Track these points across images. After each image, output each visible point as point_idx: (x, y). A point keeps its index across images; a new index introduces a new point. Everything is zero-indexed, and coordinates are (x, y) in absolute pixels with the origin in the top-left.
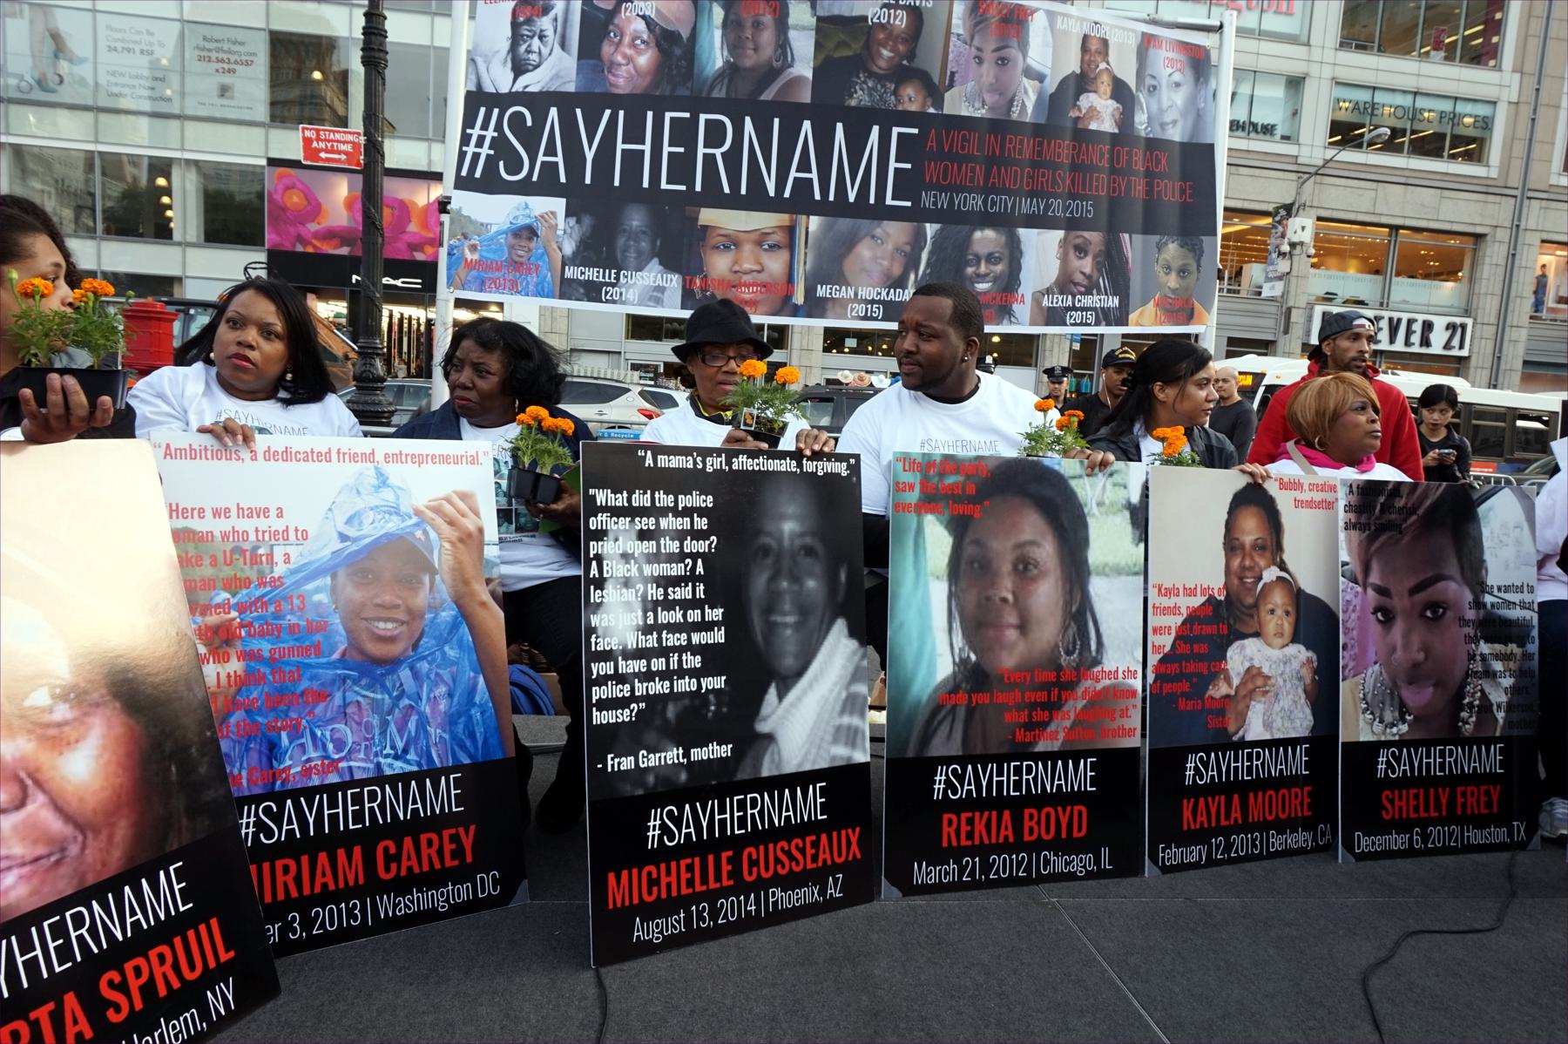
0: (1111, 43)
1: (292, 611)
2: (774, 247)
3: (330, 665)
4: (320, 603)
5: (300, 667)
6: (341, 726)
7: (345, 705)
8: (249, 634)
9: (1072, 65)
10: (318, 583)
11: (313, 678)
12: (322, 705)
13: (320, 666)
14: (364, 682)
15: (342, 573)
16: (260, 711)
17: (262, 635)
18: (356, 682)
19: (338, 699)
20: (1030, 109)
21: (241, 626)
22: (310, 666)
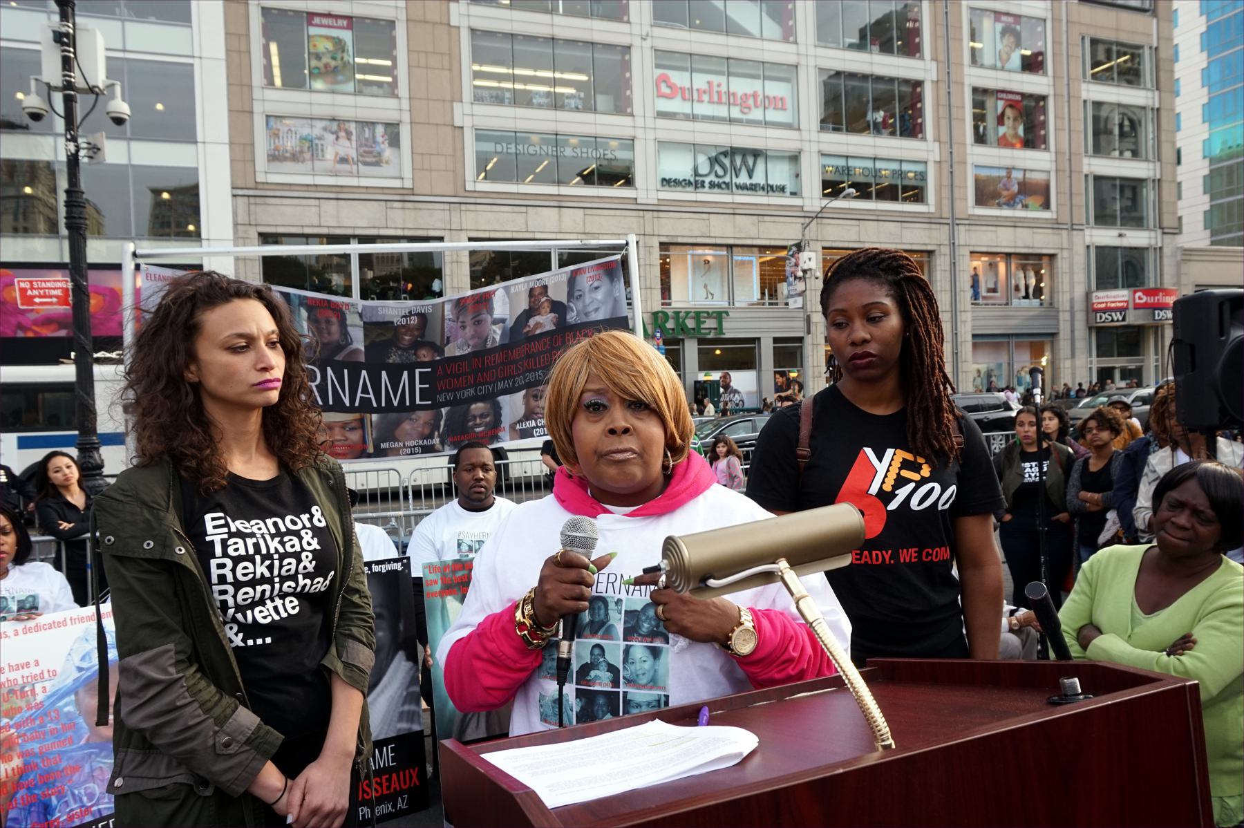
0: (550, 284)
1: (51, 721)
2: (352, 429)
3: (81, 748)
4: (69, 712)
5: (61, 754)
6: (91, 785)
7: (92, 770)
8: (24, 741)
9: (524, 305)
10: (67, 700)
11: (71, 758)
12: (77, 774)
13: (73, 750)
14: (103, 754)
15: (81, 692)
16: (36, 787)
17: (33, 739)
18: (97, 755)
19: (87, 769)
20: (498, 338)
21: (18, 737)
22: (64, 752)
